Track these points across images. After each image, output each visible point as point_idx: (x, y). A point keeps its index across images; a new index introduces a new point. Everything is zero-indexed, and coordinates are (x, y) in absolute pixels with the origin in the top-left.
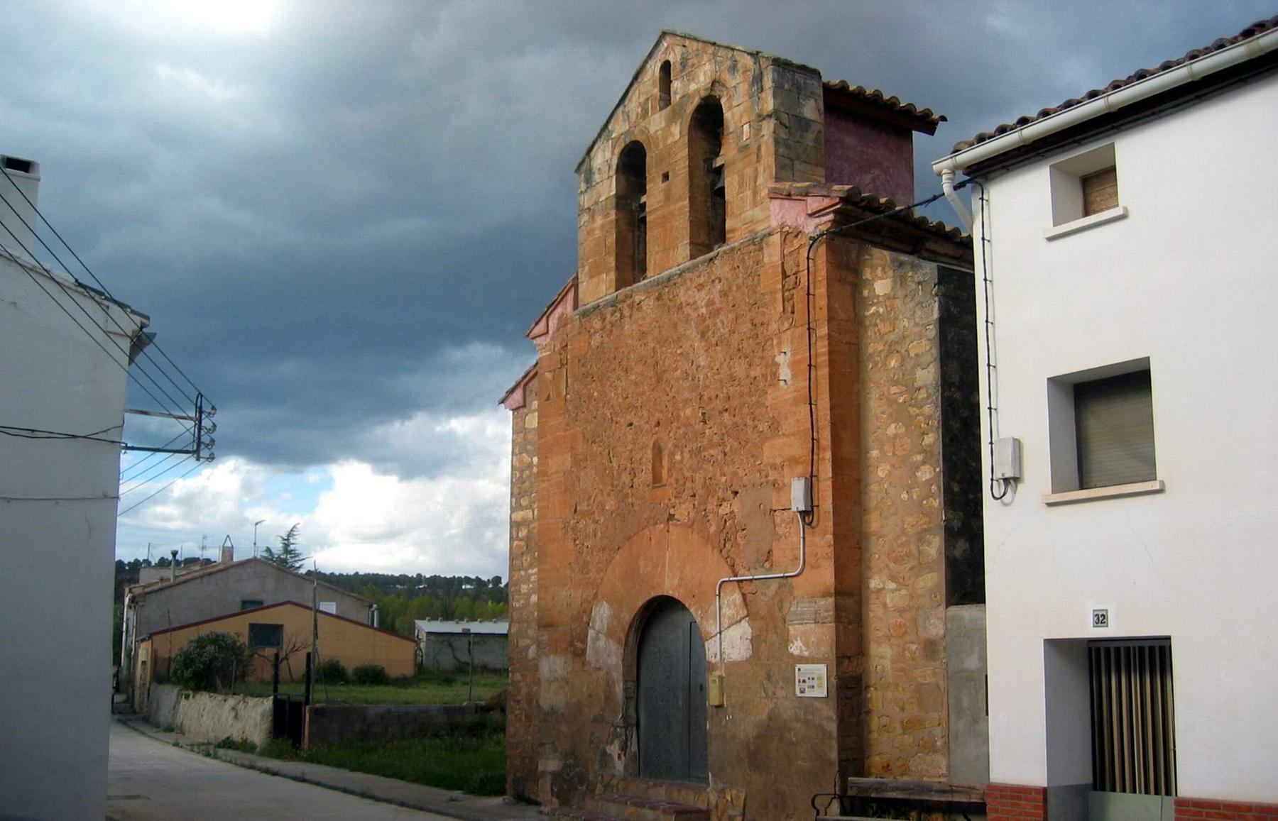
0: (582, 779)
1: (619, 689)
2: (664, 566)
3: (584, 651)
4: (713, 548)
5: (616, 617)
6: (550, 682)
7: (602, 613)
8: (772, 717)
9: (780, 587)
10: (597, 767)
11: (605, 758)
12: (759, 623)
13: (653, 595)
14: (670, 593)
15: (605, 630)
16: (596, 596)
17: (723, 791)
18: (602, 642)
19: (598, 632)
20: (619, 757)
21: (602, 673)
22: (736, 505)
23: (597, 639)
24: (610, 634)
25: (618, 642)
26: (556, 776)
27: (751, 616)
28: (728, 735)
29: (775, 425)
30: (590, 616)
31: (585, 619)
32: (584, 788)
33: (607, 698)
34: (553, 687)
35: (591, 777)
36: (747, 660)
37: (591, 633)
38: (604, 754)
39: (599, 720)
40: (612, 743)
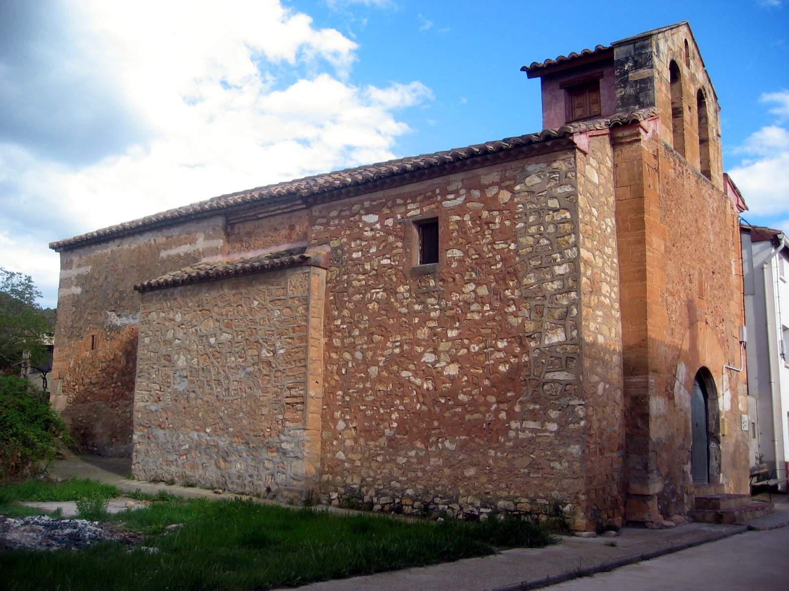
0: (674, 492)
5: (688, 374)
6: (657, 418)
7: (682, 369)
8: (737, 441)
9: (737, 375)
15: (683, 383)
16: (679, 356)
21: (682, 413)
23: (680, 388)
26: (660, 496)
29: (732, 294)
30: (676, 370)
34: (659, 420)
35: (679, 491)
37: (677, 384)
39: (682, 447)
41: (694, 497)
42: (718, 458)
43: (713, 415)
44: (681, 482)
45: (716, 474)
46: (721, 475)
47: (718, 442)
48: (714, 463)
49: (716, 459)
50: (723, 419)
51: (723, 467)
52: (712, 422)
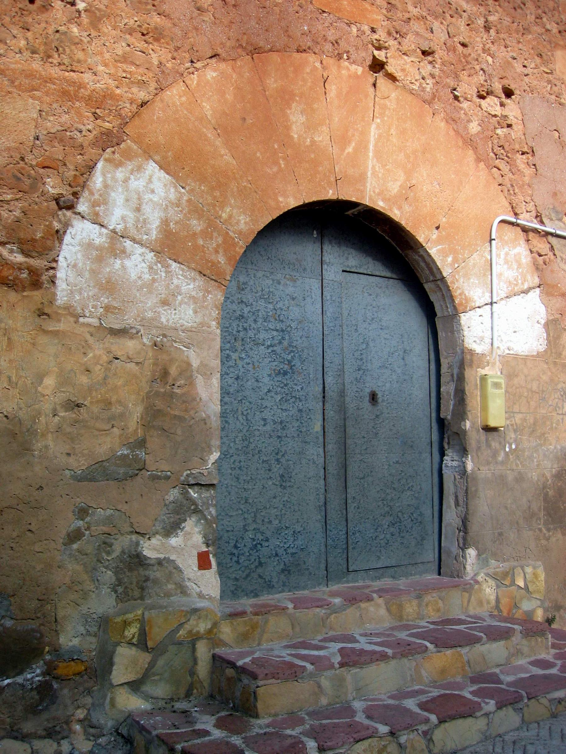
1: (208, 393)
2: (362, 146)
3: (39, 280)
4: (478, 160)
10: (103, 603)
11: (136, 574)
12: (558, 303)
13: (331, 195)
14: (380, 205)
17: (509, 574)
18: (137, 264)
19: (116, 236)
20: (203, 562)
22: (512, 109)
24: (170, 246)
25: (208, 273)
27: (547, 288)
28: (510, 477)
30: (78, 184)
31: (52, 186)
32: (34, 674)
33: (153, 416)
35: (72, 637)
36: (539, 355)
37: (80, 233)
38: (137, 560)
39: (124, 470)
40: (172, 528)
41: (203, 651)
42: (466, 497)
43: (450, 367)
44: (103, 603)
45: (455, 550)
46: (471, 552)
47: (464, 451)
48: (451, 516)
49: (457, 504)
50: (484, 378)
51: (474, 528)
52: (448, 389)
